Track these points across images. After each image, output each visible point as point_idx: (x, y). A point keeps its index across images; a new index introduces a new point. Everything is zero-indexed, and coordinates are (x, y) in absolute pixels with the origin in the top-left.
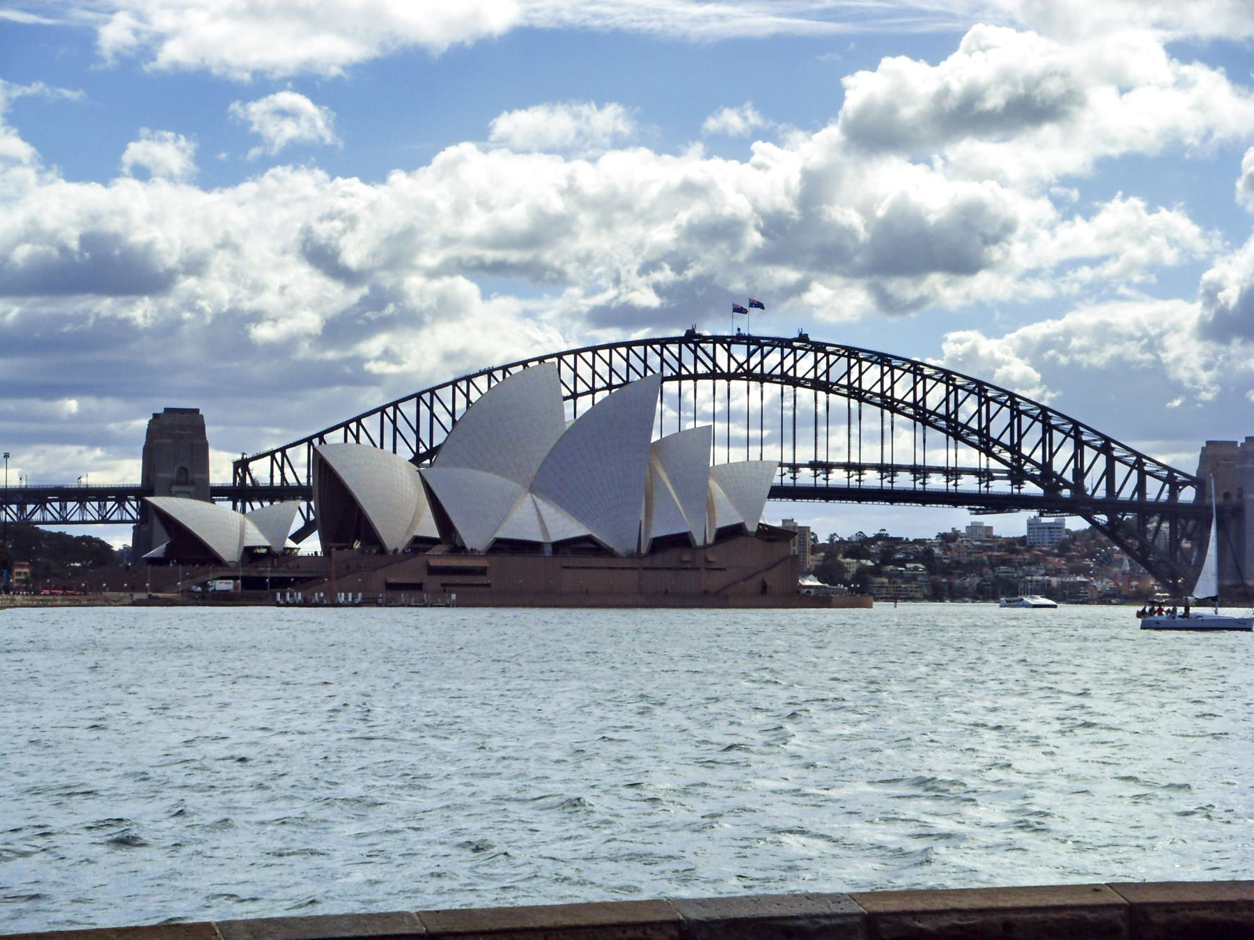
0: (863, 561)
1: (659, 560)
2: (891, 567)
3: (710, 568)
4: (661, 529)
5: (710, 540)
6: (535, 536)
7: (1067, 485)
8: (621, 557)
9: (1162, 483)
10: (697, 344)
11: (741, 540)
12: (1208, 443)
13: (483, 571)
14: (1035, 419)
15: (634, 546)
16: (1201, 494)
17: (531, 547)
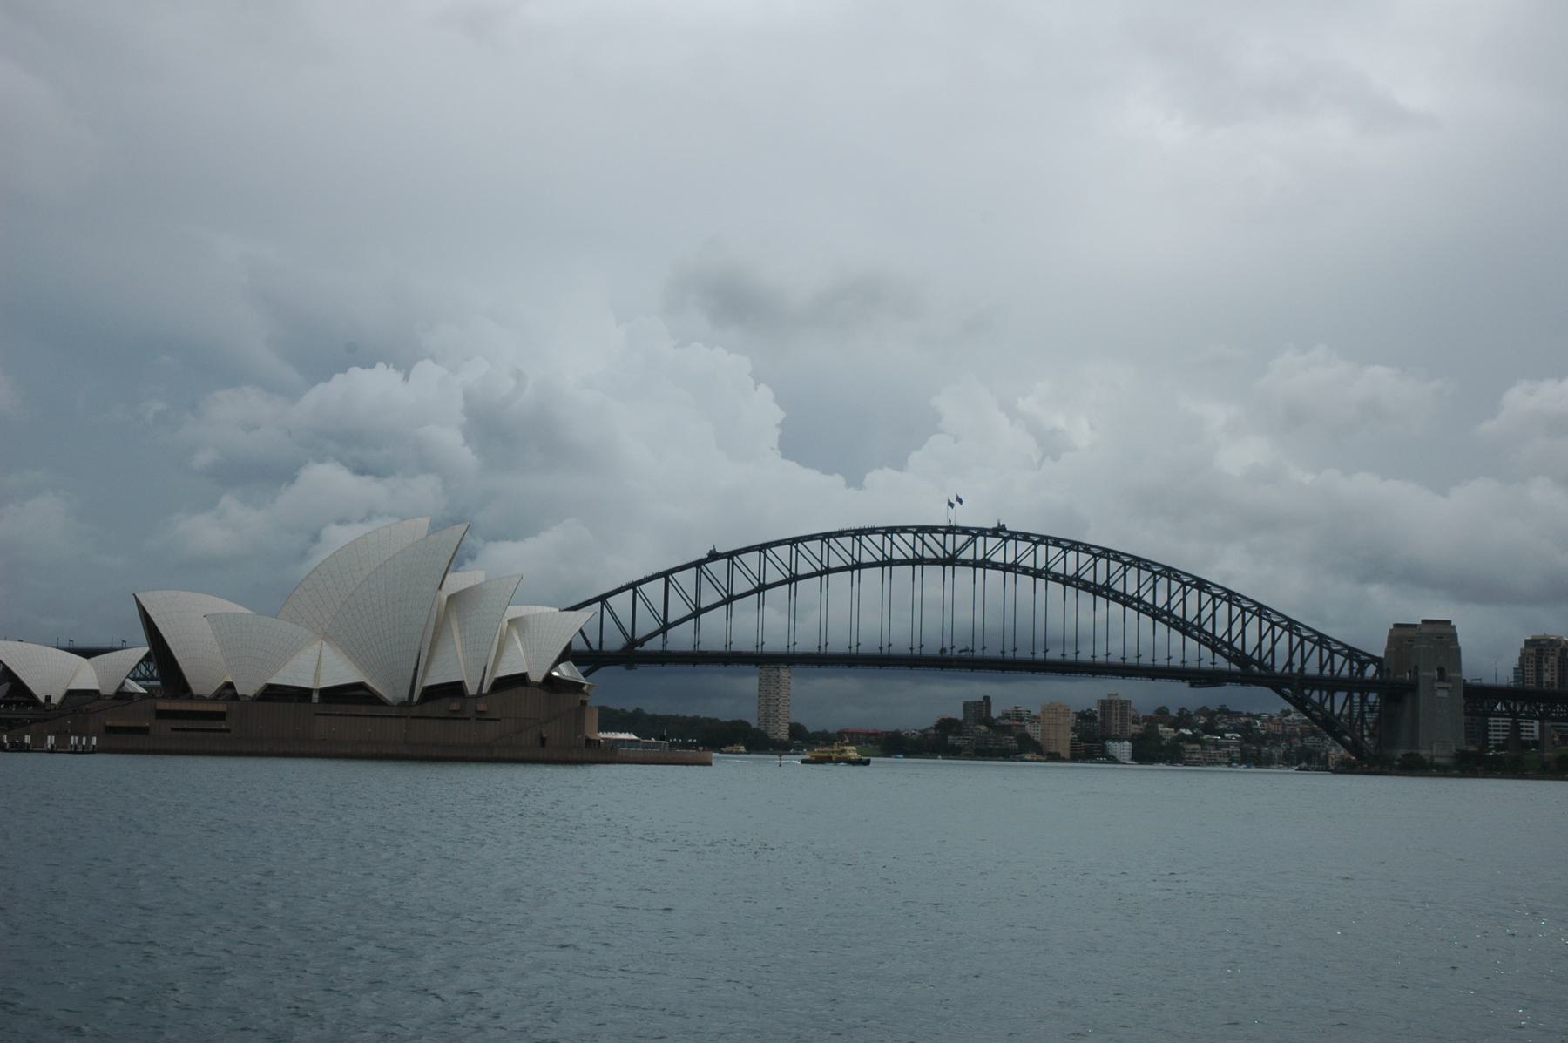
0: (1183, 731)
1: (429, 708)
2: (1208, 736)
3: (481, 717)
4: (436, 676)
5: (485, 690)
6: (306, 683)
7: (1254, 662)
8: (393, 706)
9: (1343, 658)
10: (915, 534)
11: (522, 690)
12: (1396, 626)
13: (221, 716)
14: (1223, 599)
15: (404, 694)
16: (1380, 670)
17: (303, 694)
